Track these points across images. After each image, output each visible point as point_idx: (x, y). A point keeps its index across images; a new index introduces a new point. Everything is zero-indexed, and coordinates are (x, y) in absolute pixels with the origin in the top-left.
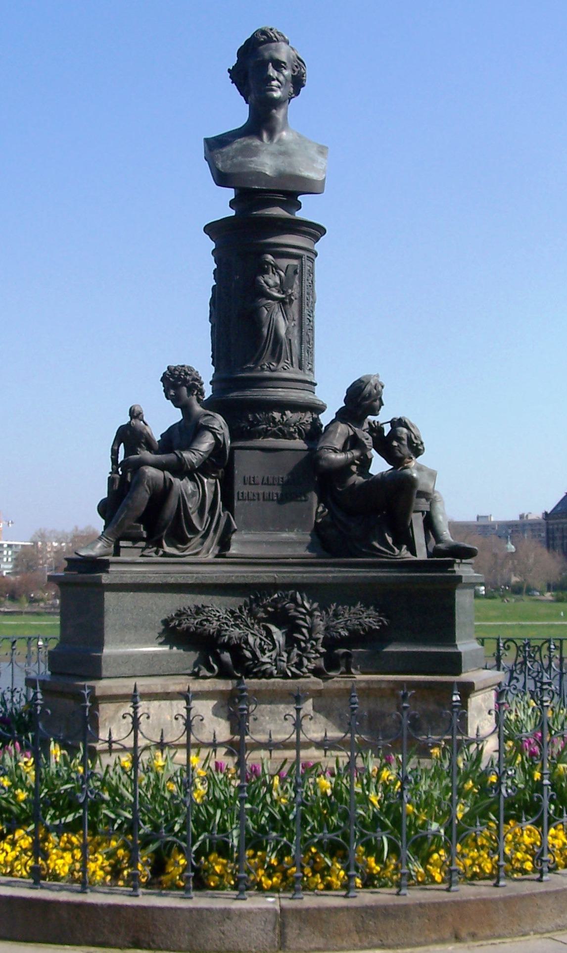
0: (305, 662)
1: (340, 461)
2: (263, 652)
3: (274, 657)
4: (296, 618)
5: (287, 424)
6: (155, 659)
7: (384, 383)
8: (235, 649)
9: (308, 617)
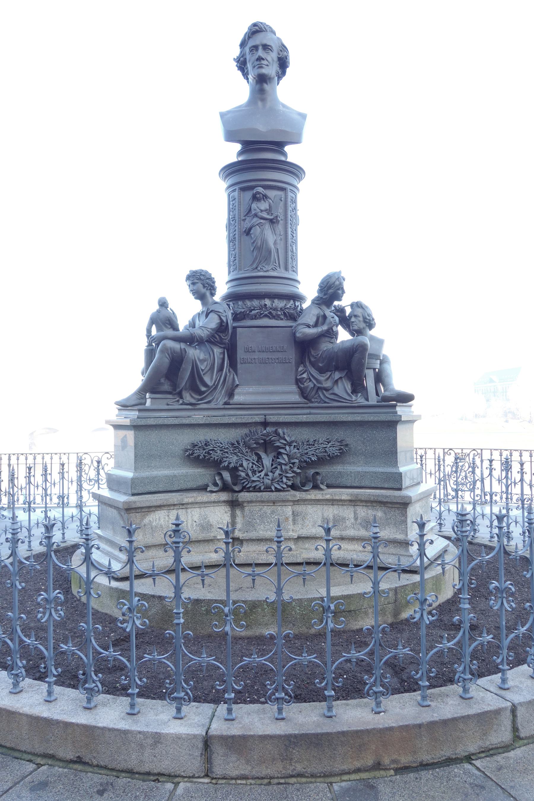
0: (284, 480)
2: (254, 472)
3: (262, 476)
5: (275, 309)
6: (174, 479)
7: (345, 277)
8: (234, 471)
9: (287, 448)
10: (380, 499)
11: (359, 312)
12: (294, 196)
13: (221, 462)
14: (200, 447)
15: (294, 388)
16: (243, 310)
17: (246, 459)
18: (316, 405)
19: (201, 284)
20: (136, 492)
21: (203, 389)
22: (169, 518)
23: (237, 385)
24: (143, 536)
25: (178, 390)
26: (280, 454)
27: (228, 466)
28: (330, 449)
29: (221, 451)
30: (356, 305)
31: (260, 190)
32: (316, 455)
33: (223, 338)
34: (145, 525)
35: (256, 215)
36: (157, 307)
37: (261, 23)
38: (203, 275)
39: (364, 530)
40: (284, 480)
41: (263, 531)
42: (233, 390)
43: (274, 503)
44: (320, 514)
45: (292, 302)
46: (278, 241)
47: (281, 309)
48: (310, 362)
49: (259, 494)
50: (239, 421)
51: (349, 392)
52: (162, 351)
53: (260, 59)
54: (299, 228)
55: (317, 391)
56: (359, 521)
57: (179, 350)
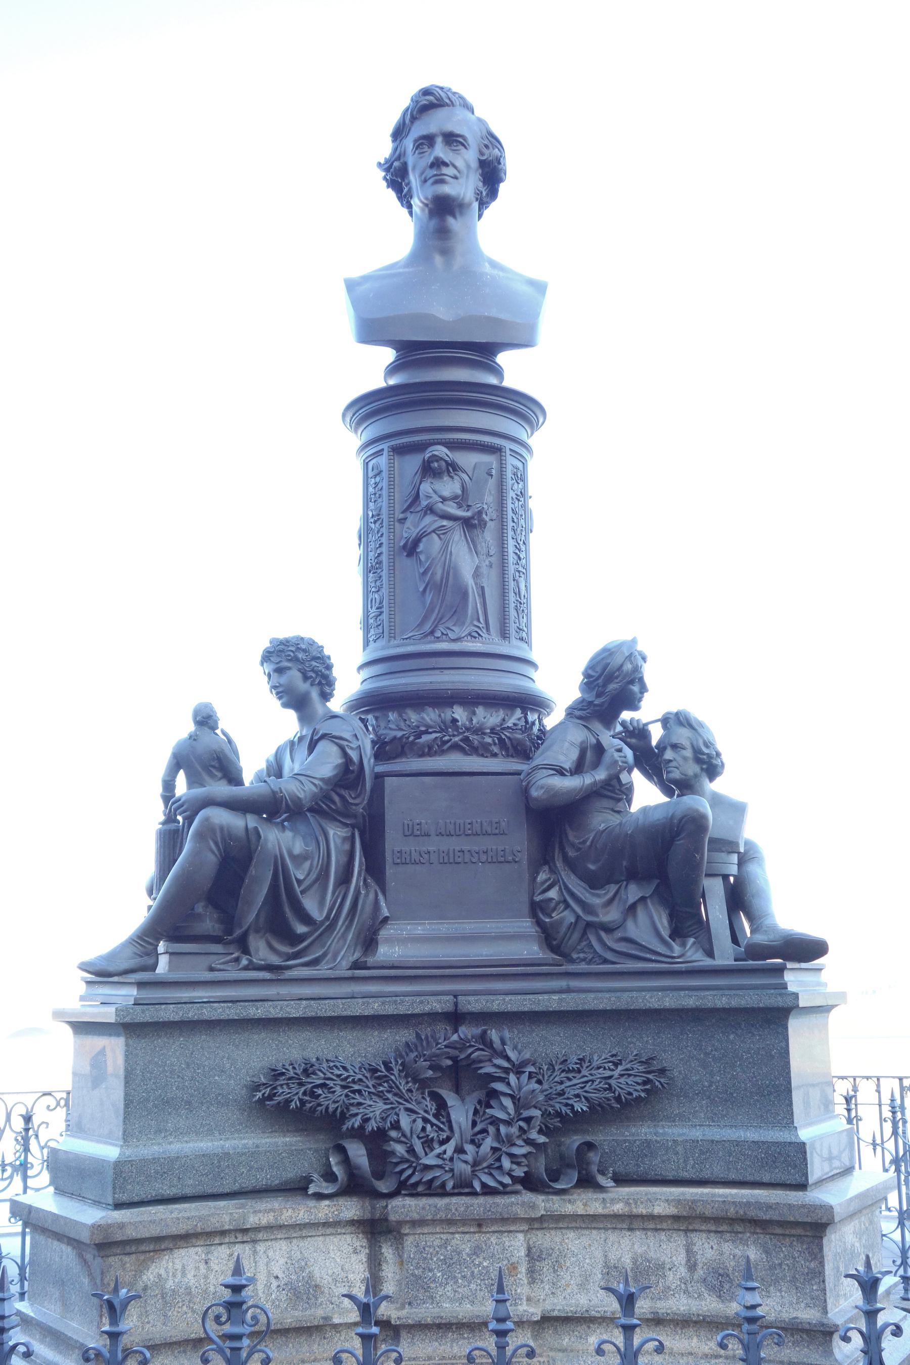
0: (506, 1163)
1: (570, 792)
2: (428, 1144)
3: (449, 1153)
4: (492, 1078)
5: (479, 731)
6: (224, 1164)
7: (647, 652)
8: (376, 1141)
9: (512, 1078)
10: (752, 1213)
11: (682, 735)
12: (520, 465)
13: (344, 1117)
14: (290, 1079)
15: (526, 925)
16: (399, 734)
17: (407, 1110)
18: (583, 967)
19: (297, 670)
20: (125, 1198)
21: (301, 929)
22: (209, 1269)
23: (386, 919)
24: (140, 1316)
25: (238, 932)
26: (494, 1094)
27: (362, 1127)
28: (622, 1080)
29: (344, 1087)
30: (676, 721)
31: (441, 451)
32: (586, 1098)
33: (351, 801)
34: (145, 1288)
35: (430, 510)
36: (188, 727)
37: (442, 88)
38: (304, 651)
39: (714, 1298)
40: (506, 1163)
41: (452, 1300)
42: (375, 932)
43: (480, 1225)
44: (599, 1254)
45: (518, 713)
46: (484, 570)
47: (493, 730)
48: (566, 859)
49: (441, 1202)
50: (390, 1010)
51: (665, 934)
52: (200, 836)
53: (438, 163)
54: (534, 539)
55: (584, 933)
56: (700, 1272)
57: (241, 833)
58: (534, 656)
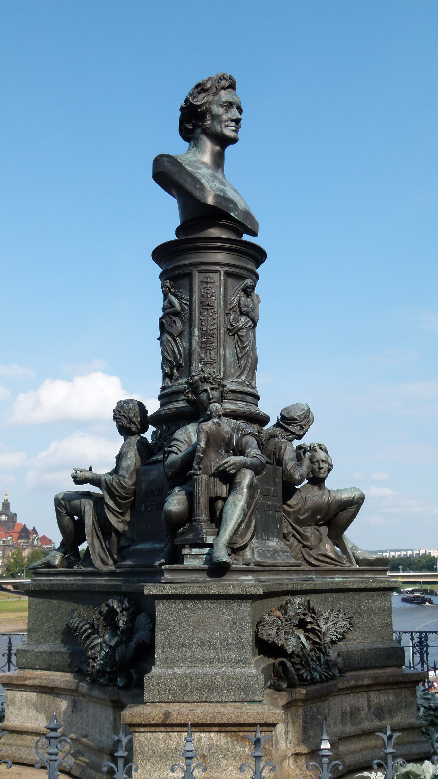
39: (378, 721)
44: (339, 707)
56: (372, 709)
58: (259, 394)
